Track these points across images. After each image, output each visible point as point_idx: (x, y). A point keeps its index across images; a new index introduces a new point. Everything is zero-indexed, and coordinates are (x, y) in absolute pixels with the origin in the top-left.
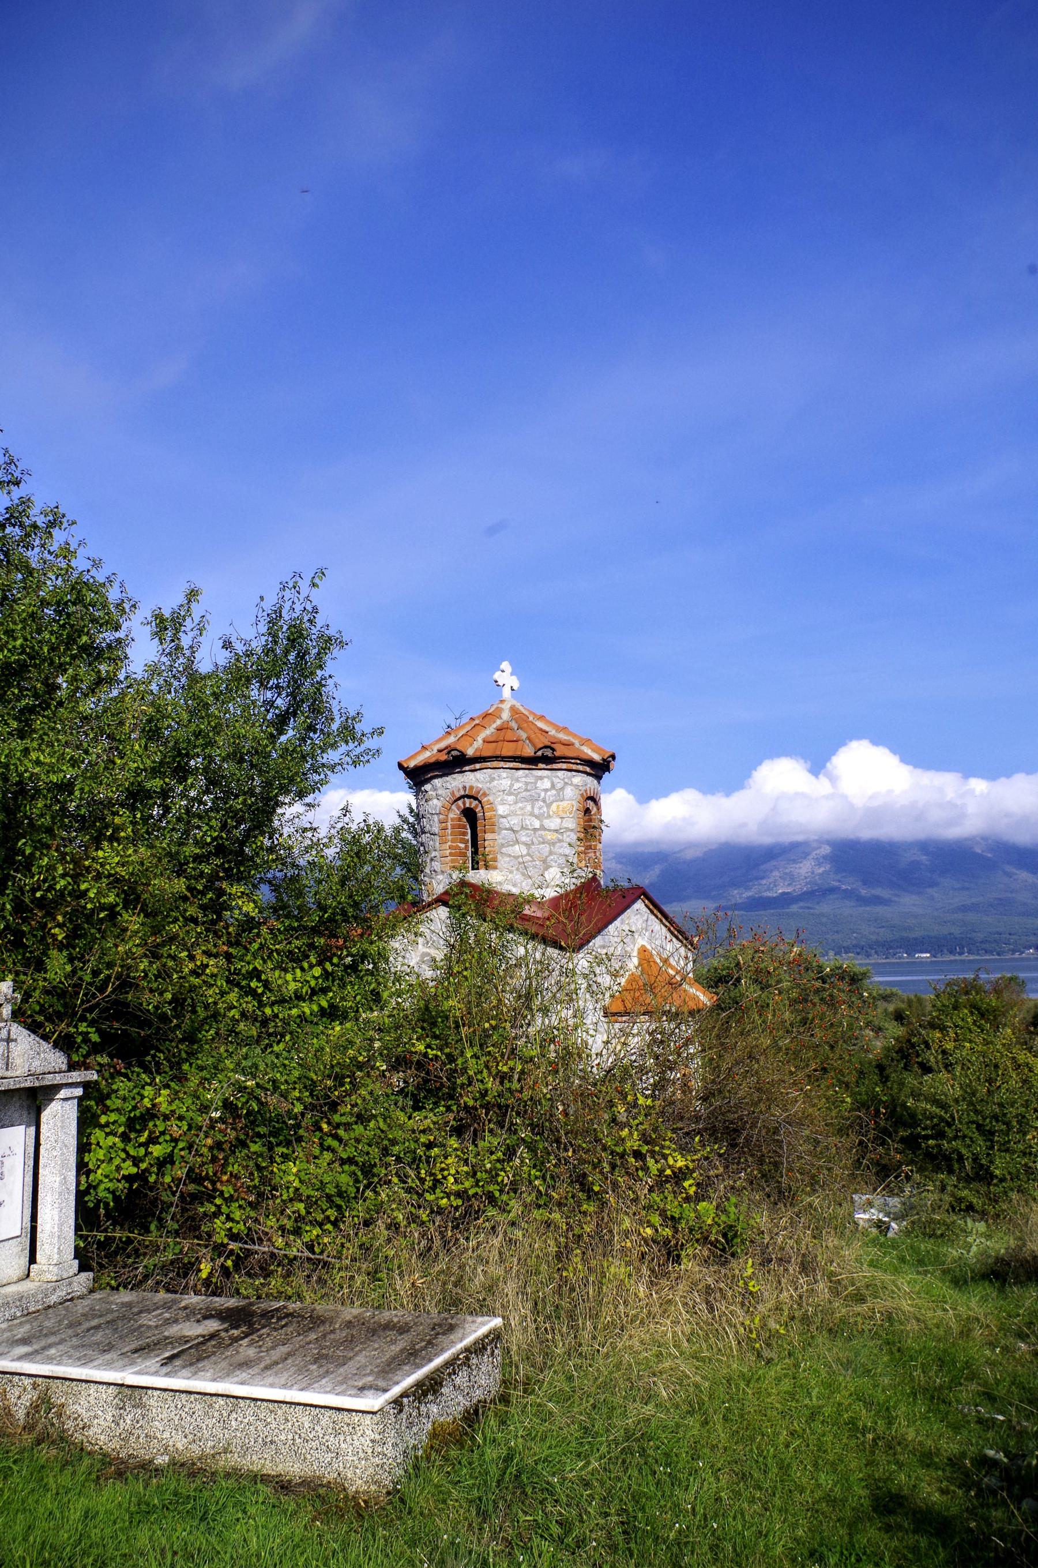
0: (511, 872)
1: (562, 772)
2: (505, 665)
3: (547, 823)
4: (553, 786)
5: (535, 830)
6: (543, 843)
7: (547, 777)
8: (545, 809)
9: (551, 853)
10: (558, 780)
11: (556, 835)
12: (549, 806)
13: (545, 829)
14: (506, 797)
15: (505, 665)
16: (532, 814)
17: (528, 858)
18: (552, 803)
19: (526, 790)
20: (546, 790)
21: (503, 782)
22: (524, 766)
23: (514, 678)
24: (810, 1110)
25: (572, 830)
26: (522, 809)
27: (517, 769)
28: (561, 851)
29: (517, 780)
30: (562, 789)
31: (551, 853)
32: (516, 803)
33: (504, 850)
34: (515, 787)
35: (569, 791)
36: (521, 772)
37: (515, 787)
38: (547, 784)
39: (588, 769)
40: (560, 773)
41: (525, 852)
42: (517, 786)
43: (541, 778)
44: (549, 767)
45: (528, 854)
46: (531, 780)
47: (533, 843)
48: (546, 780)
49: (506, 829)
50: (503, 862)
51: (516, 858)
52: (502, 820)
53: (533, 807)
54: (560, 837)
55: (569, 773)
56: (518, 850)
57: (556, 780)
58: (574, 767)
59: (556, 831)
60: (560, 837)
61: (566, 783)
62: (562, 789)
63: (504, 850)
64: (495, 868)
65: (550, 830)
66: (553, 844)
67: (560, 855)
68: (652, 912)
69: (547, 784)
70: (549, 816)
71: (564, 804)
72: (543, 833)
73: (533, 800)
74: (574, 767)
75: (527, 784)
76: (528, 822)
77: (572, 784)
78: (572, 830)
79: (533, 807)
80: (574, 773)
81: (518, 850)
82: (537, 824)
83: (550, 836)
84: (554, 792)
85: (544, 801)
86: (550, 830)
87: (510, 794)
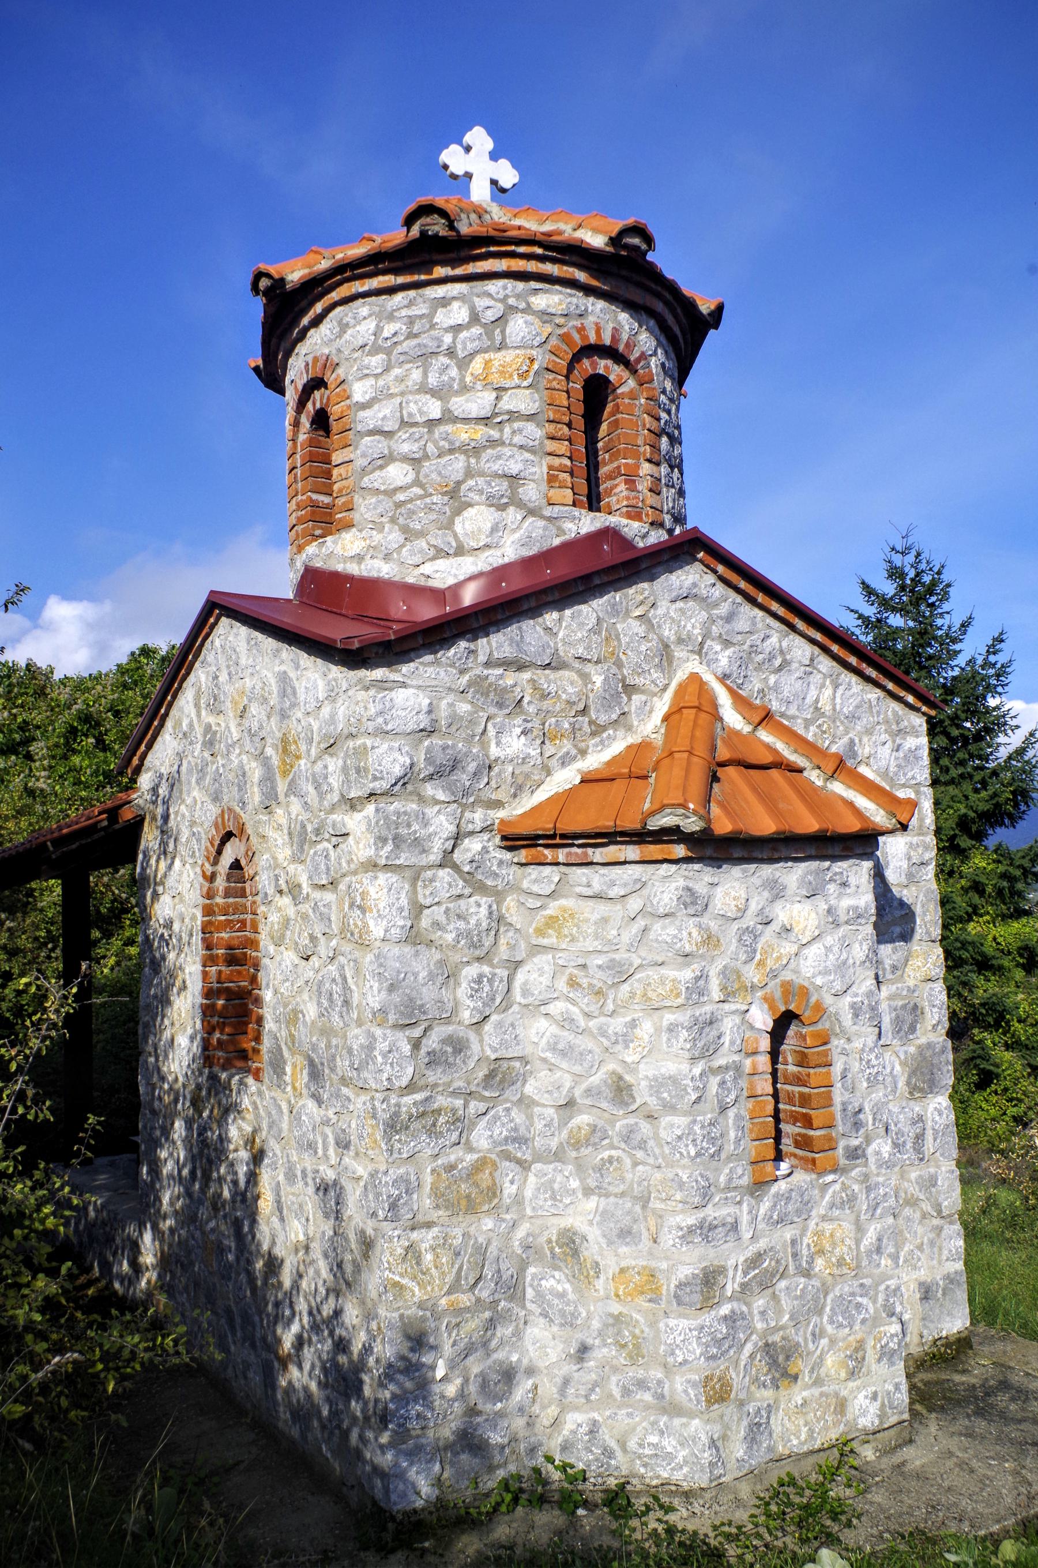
0: (380, 528)
1: (500, 283)
2: (479, 138)
3: (460, 405)
4: (475, 318)
5: (431, 423)
6: (451, 451)
7: (461, 298)
8: (454, 372)
9: (469, 474)
10: (487, 302)
11: (480, 433)
12: (463, 364)
13: (456, 420)
14: (366, 360)
15: (479, 138)
16: (423, 389)
17: (417, 491)
18: (472, 355)
19: (411, 336)
20: (457, 329)
21: (362, 328)
22: (401, 280)
23: (504, 164)
24: (906, 1130)
25: (531, 417)
26: (400, 380)
27: (391, 291)
28: (497, 467)
29: (391, 317)
30: (501, 320)
31: (469, 474)
32: (387, 370)
33: (366, 482)
34: (386, 334)
35: (518, 327)
36: (399, 298)
37: (386, 334)
38: (459, 313)
39: (581, 276)
40: (494, 287)
41: (411, 477)
42: (388, 330)
43: (444, 302)
44: (459, 271)
45: (417, 482)
46: (421, 309)
47: (427, 457)
48: (456, 305)
49: (371, 433)
50: (365, 508)
51: (391, 493)
52: (362, 414)
53: (425, 374)
54: (495, 434)
55: (520, 286)
56: (397, 474)
57: (481, 303)
58: (532, 266)
59: (485, 420)
60: (495, 434)
61: (513, 309)
62: (501, 320)
63: (366, 482)
64: (349, 525)
65: (466, 420)
66: (474, 450)
67: (496, 475)
68: (752, 601)
69: (459, 313)
70: (464, 389)
71: (507, 356)
72: (449, 428)
73: (425, 357)
74: (532, 266)
75: (411, 321)
76: (413, 408)
77: (528, 310)
78: (531, 417)
79: (425, 374)
80: (534, 285)
81: (397, 474)
82: (434, 409)
83: (463, 434)
84: (476, 330)
85: (451, 353)
86: (466, 420)
87: (376, 350)
